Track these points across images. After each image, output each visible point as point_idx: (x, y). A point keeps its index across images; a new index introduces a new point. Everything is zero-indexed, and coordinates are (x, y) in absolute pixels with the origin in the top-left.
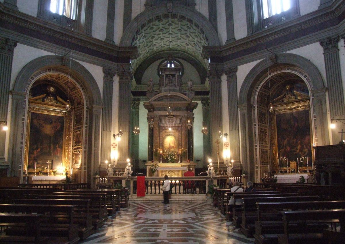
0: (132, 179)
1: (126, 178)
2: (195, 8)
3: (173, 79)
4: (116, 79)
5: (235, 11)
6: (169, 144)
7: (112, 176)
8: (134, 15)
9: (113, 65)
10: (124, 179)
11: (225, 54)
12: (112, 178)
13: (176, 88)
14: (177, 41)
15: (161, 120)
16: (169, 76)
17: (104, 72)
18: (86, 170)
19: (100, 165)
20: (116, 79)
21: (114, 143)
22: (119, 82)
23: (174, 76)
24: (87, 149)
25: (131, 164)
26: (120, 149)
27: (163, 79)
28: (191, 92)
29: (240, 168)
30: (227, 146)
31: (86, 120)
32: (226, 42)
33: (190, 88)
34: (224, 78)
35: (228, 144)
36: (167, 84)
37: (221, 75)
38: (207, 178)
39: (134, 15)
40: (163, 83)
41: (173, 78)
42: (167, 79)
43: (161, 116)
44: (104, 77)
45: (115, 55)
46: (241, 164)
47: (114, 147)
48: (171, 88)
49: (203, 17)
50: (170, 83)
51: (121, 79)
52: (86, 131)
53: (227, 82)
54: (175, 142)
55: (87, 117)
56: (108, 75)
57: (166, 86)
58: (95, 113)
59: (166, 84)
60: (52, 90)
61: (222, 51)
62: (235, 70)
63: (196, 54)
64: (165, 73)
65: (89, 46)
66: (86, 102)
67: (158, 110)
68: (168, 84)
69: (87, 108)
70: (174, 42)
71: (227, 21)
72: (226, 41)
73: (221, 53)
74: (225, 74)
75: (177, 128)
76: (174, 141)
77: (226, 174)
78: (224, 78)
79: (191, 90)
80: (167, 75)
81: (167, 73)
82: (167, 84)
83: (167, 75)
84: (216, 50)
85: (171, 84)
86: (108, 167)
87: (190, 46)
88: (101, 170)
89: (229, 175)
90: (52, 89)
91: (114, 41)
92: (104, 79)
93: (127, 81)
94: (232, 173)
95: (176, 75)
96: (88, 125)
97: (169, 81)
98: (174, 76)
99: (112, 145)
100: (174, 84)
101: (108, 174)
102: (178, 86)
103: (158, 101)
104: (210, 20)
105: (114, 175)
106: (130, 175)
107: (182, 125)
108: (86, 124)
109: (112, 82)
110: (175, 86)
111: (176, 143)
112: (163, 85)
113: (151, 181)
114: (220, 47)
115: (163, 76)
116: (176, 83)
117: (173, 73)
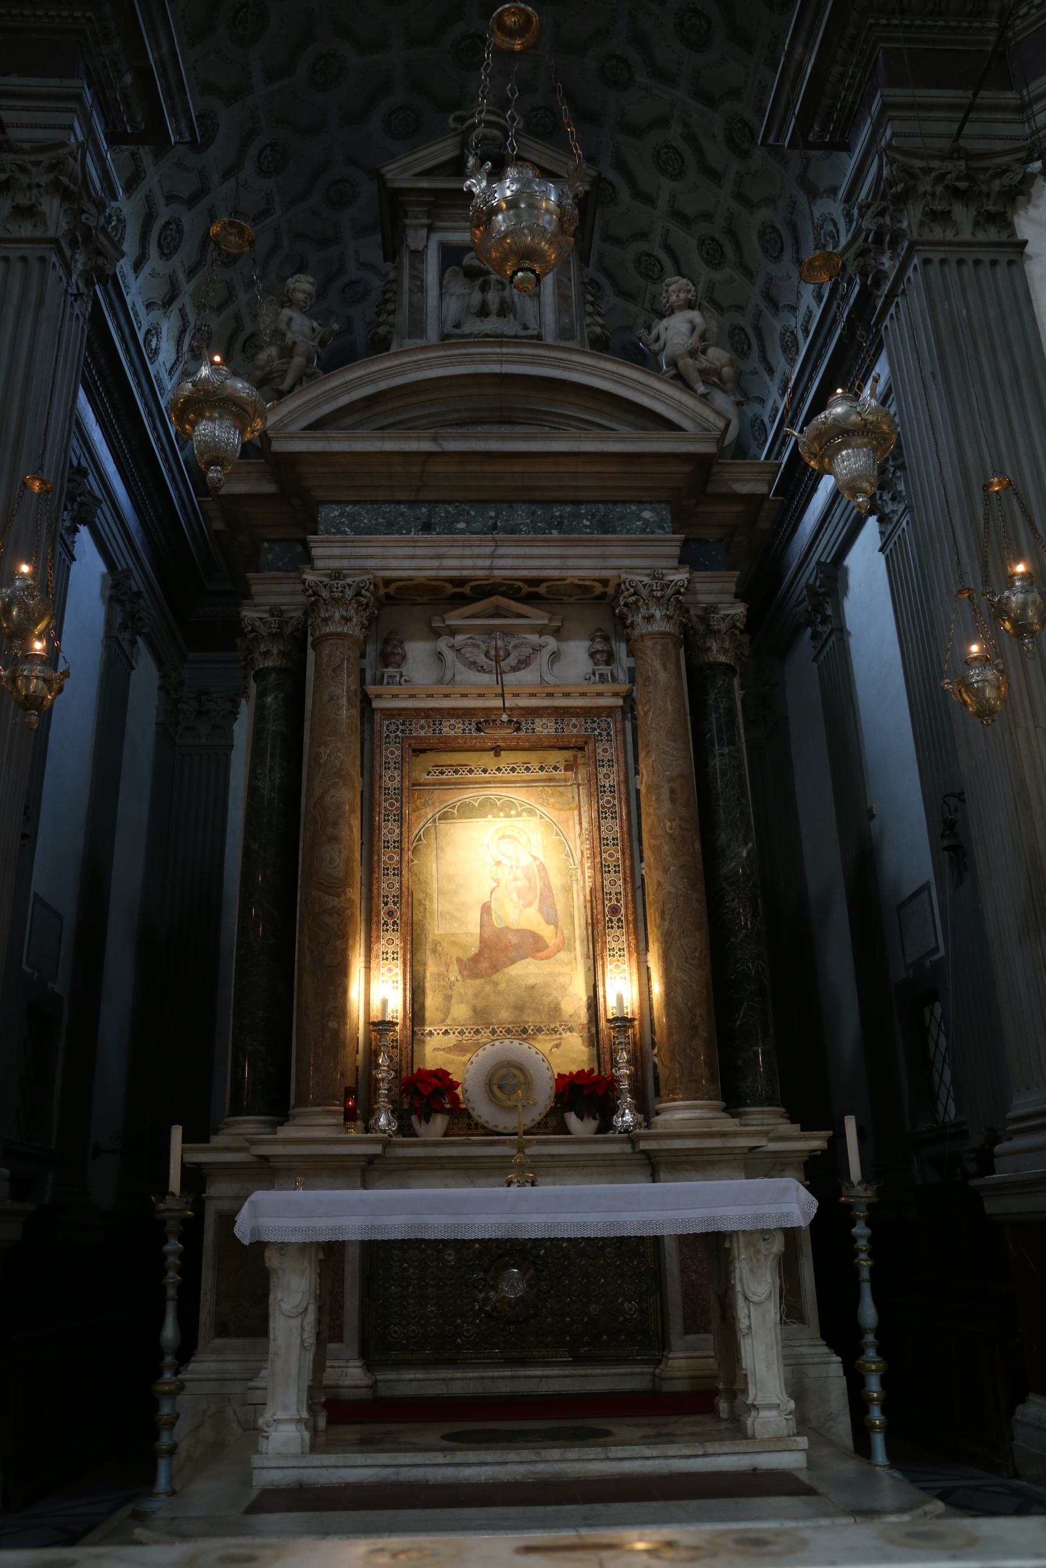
6: (486, 909)
27: (418, 279)
28: (701, 389)
33: (693, 353)
36: (457, 326)
40: (418, 311)
42: (458, 287)
50: (483, 312)
54: (556, 880)
59: (450, 322)
64: (436, 238)
68: (475, 326)
75: (573, 729)
76: (542, 868)
79: (705, 374)
82: (457, 326)
83: (450, 255)
97: (476, 297)
107: (628, 697)
111: (568, 890)
115: (419, 256)
116: (550, 317)
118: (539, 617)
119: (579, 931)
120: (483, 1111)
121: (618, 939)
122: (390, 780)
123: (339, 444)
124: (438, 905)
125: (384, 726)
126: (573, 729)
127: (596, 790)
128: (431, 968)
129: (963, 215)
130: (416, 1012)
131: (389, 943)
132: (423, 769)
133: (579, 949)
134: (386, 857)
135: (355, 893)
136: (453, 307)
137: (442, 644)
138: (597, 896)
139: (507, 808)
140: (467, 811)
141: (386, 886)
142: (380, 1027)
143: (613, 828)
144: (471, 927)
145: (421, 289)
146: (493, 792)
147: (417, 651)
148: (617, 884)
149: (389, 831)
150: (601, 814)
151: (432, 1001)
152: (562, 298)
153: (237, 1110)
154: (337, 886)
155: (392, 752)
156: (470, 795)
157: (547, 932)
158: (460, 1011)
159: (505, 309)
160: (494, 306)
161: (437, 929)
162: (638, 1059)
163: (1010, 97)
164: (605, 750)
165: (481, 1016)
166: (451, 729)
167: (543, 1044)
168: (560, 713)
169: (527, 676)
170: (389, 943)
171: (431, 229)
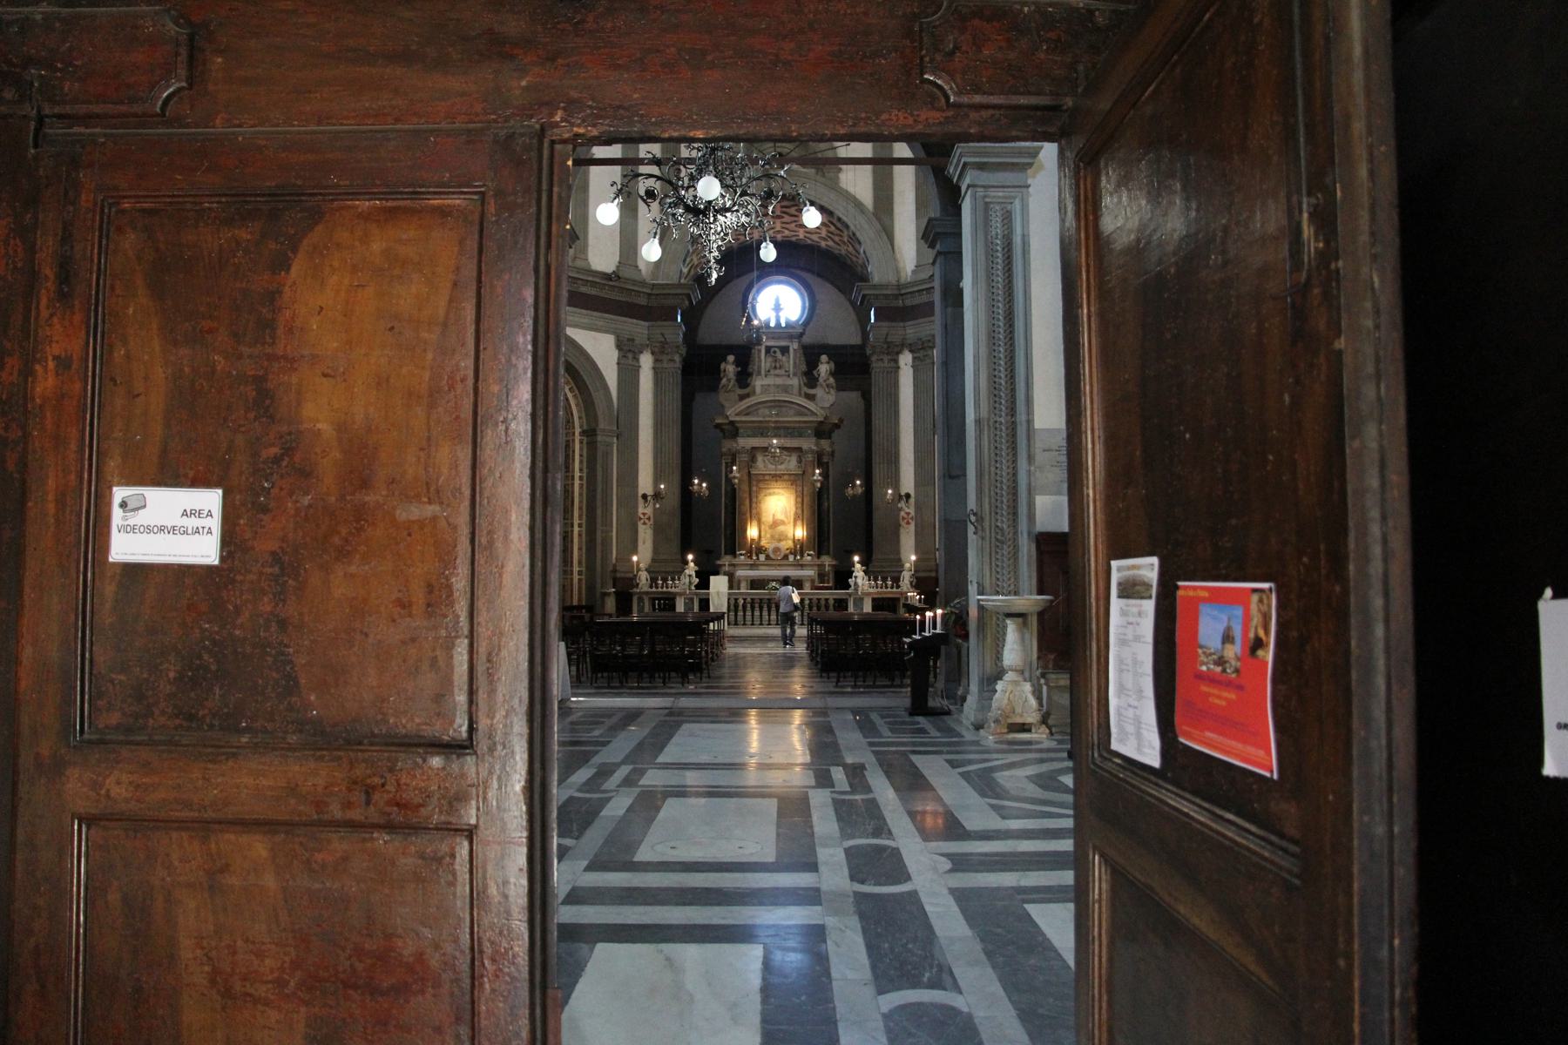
0: (697, 594)
1: (684, 594)
2: (838, 178)
3: (784, 359)
4: (646, 361)
7: (646, 589)
9: (638, 328)
10: (680, 594)
11: (909, 302)
12: (647, 593)
13: (789, 382)
14: (797, 229)
15: (753, 459)
16: (775, 352)
17: (619, 346)
18: (583, 577)
19: (615, 565)
20: (646, 361)
21: (644, 514)
22: (654, 368)
24: (584, 529)
25: (696, 565)
26: (658, 531)
27: (759, 357)
29: (933, 574)
30: (908, 523)
31: (581, 462)
32: (913, 272)
34: (906, 359)
35: (912, 518)
37: (898, 353)
38: (850, 595)
40: (760, 367)
41: (783, 355)
42: (770, 359)
43: (753, 448)
44: (619, 359)
45: (643, 301)
46: (937, 565)
47: (644, 523)
48: (779, 381)
49: (858, 205)
50: (775, 368)
51: (656, 361)
52: (581, 486)
53: (911, 370)
55: (581, 456)
56: (628, 351)
58: (601, 449)
61: (902, 295)
62: (931, 344)
63: (849, 262)
65: (583, 289)
66: (580, 418)
67: (748, 436)
68: (772, 372)
69: (583, 433)
70: (787, 232)
72: (913, 268)
73: (900, 298)
77: (898, 587)
78: (906, 359)
79: (828, 386)
80: (768, 349)
83: (768, 349)
84: (889, 292)
85: (777, 372)
86: (639, 570)
87: (830, 243)
88: (618, 575)
89: (905, 589)
91: (637, 267)
92: (618, 364)
93: (671, 365)
94: (911, 583)
95: (791, 350)
96: (585, 475)
98: (785, 350)
99: (640, 519)
101: (638, 584)
102: (795, 374)
103: (747, 414)
104: (875, 214)
105: (651, 587)
106: (693, 588)
107: (804, 472)
108: (581, 470)
109: (636, 369)
112: (759, 373)
113: (736, 600)
114: (899, 286)
115: (760, 351)
117: (783, 343)
118: (785, 453)
119: (792, 520)
120: (772, 556)
121: (799, 523)
122: (754, 488)
123: (744, 419)
124: (764, 514)
125: (753, 477)
126: (792, 478)
127: (796, 492)
128: (763, 527)
129: (886, 358)
130: (760, 536)
131: (755, 523)
132: (761, 485)
133: (792, 524)
134: (754, 505)
135: (748, 515)
136: (768, 365)
137: (765, 459)
138: (796, 513)
139: (778, 494)
140: (770, 494)
141: (754, 511)
142: (752, 540)
143: (799, 500)
144: (770, 519)
145: (760, 361)
146: (776, 490)
147: (760, 458)
148: (800, 512)
149: (754, 500)
150: (797, 497)
151: (763, 534)
152: (795, 363)
153: (726, 554)
154: (745, 514)
155: (754, 483)
156: (771, 491)
157: (785, 520)
158: (768, 536)
159: (780, 368)
160: (778, 365)
161: (764, 519)
162: (801, 547)
163: (902, 324)
164: (799, 483)
165: (772, 537)
166: (767, 477)
167: (783, 543)
168: (790, 475)
169: (783, 467)
170: (755, 523)
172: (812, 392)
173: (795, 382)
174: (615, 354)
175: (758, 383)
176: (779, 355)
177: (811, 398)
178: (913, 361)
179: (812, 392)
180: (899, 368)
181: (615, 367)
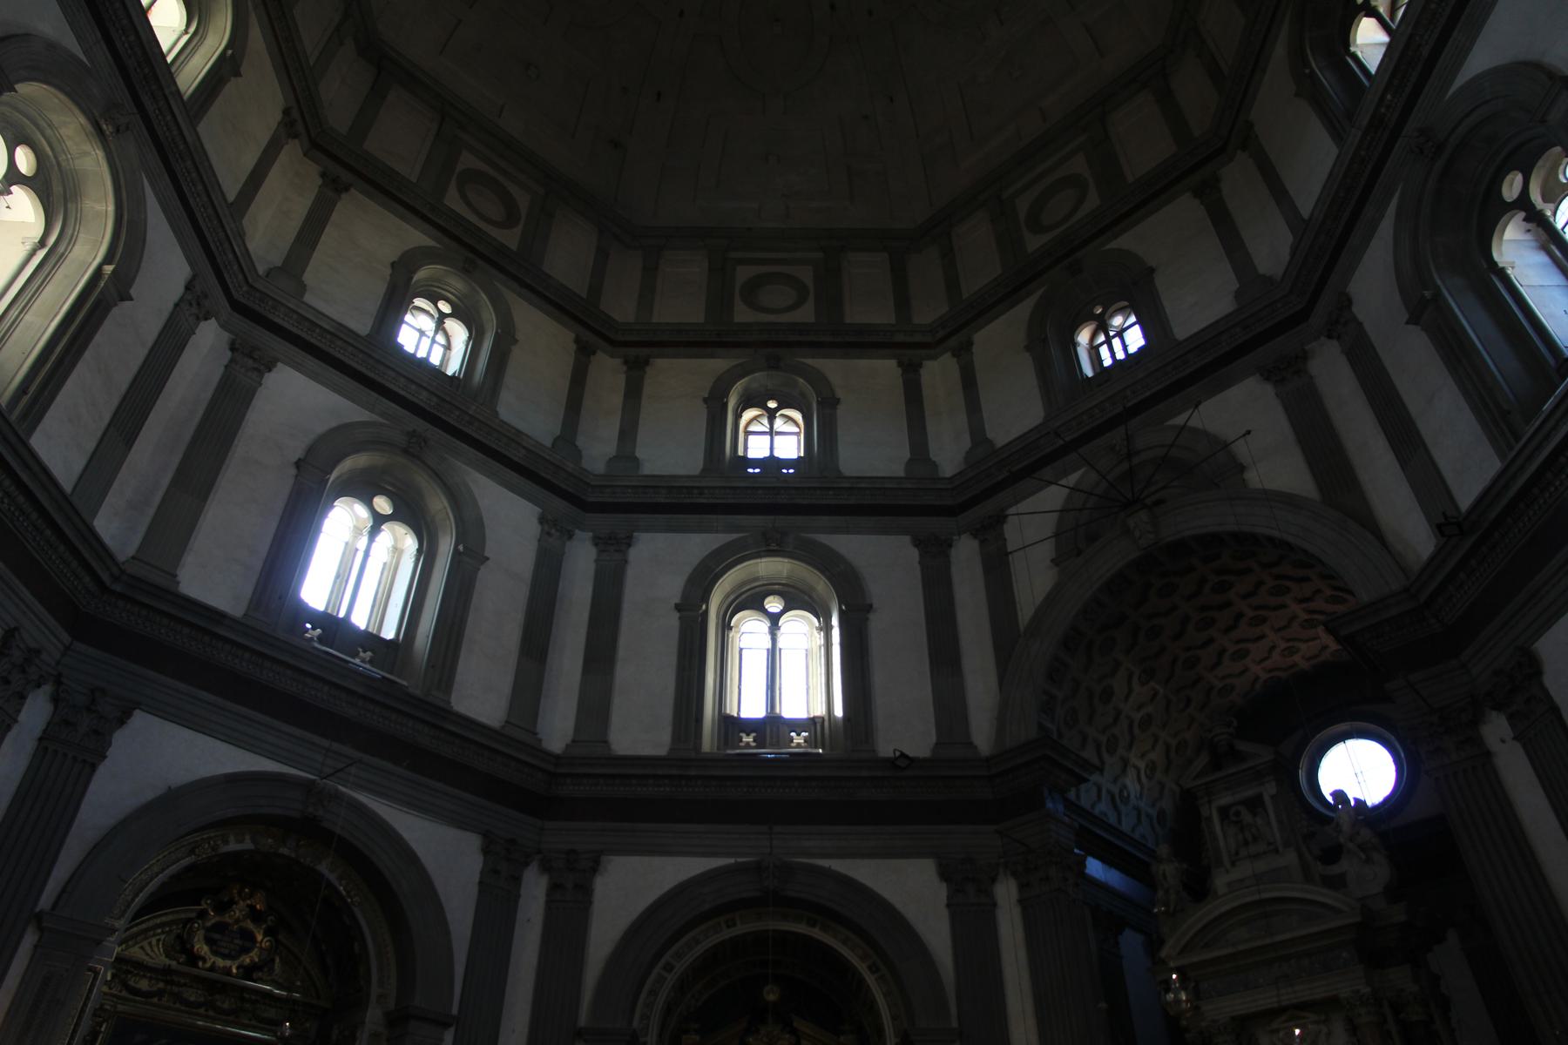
4: (1006, 893)
5: (1414, 404)
8: (1025, 613)
16: (1238, 814)
17: (945, 874)
20: (1006, 893)
22: (1020, 901)
23: (1255, 804)
34: (1496, 730)
36: (1237, 853)
39: (1025, 613)
44: (948, 897)
49: (1290, 501)
50: (1246, 843)
51: (1022, 887)
57: (1233, 864)
60: (771, 997)
71: (1403, 463)
74: (1494, 714)
78: (1496, 730)
80: (1224, 812)
81: (1225, 800)
82: (1237, 853)
83: (1224, 812)
90: (771, 995)
91: (971, 743)
92: (948, 906)
95: (1267, 798)
98: (1255, 804)
100: (1269, 844)
110: (1277, 851)
117: (1250, 793)
171: (1210, 802)
172: (1335, 869)
173: (1290, 858)
174: (942, 891)
175: (1220, 881)
176: (1247, 817)
177: (1336, 883)
178: (1513, 726)
179: (1335, 869)
180: (1488, 754)
181: (945, 913)
